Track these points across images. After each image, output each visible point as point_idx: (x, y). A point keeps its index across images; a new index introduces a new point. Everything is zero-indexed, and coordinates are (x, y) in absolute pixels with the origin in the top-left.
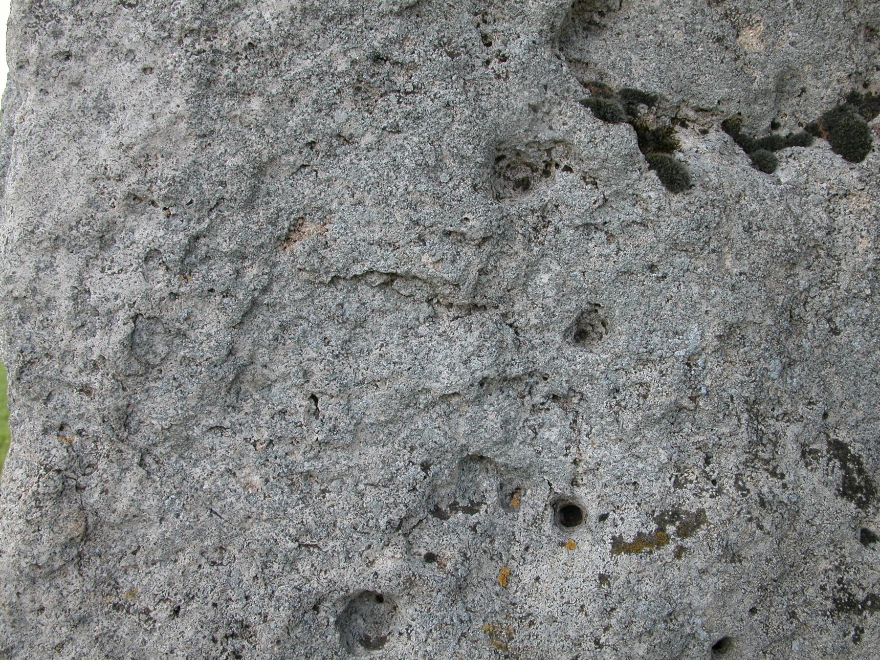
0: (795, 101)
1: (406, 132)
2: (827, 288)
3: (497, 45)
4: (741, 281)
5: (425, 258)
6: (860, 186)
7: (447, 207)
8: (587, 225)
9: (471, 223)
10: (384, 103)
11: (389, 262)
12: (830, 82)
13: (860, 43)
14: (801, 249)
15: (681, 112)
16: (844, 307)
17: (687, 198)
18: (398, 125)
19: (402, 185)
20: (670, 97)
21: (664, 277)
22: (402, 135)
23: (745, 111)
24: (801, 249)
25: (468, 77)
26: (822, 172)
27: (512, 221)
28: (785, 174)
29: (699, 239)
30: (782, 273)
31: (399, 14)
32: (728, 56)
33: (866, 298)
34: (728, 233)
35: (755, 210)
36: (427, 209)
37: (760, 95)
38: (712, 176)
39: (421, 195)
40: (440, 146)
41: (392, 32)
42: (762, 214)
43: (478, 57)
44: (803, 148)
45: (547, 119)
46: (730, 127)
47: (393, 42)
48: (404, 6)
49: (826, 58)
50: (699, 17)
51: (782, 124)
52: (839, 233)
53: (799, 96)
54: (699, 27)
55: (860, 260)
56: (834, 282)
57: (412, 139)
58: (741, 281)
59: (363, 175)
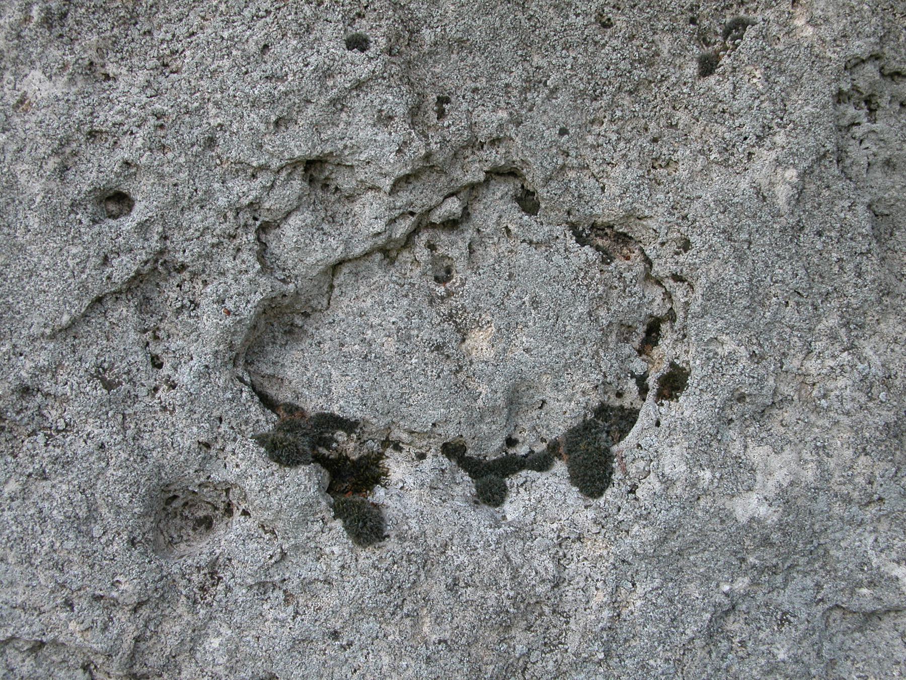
0: (535, 414)
1: (54, 479)
2: (551, 651)
3: (166, 370)
4: (438, 652)
5: (72, 626)
6: (595, 529)
7: (97, 567)
8: (262, 584)
9: (122, 587)
10: (30, 446)
11: (35, 628)
12: (573, 395)
13: (611, 346)
14: (518, 608)
15: (392, 434)
16: (573, 673)
17: (378, 552)
18: (44, 472)
19: (47, 541)
20: (374, 420)
21: (350, 644)
22: (49, 483)
23: (467, 433)
24: (518, 608)
25: (130, 411)
26: (552, 510)
27: (174, 581)
28: (512, 509)
29: (390, 602)
30: (494, 637)
31: (53, 337)
32: (448, 367)
33: (599, 663)
34: (427, 593)
35: (463, 563)
36: (76, 570)
37: (487, 413)
38: (413, 522)
39: (69, 553)
40: (92, 494)
41: (43, 359)
42: (471, 567)
43: (143, 385)
44: (539, 474)
45: (221, 456)
46: (454, 450)
47: (43, 370)
48: (57, 328)
49: (566, 366)
50: (416, 321)
51: (521, 440)
52: (569, 584)
53: (540, 408)
54: (416, 332)
55: (593, 617)
56: (561, 643)
57: (61, 488)
58: (438, 652)
59: (5, 529)
